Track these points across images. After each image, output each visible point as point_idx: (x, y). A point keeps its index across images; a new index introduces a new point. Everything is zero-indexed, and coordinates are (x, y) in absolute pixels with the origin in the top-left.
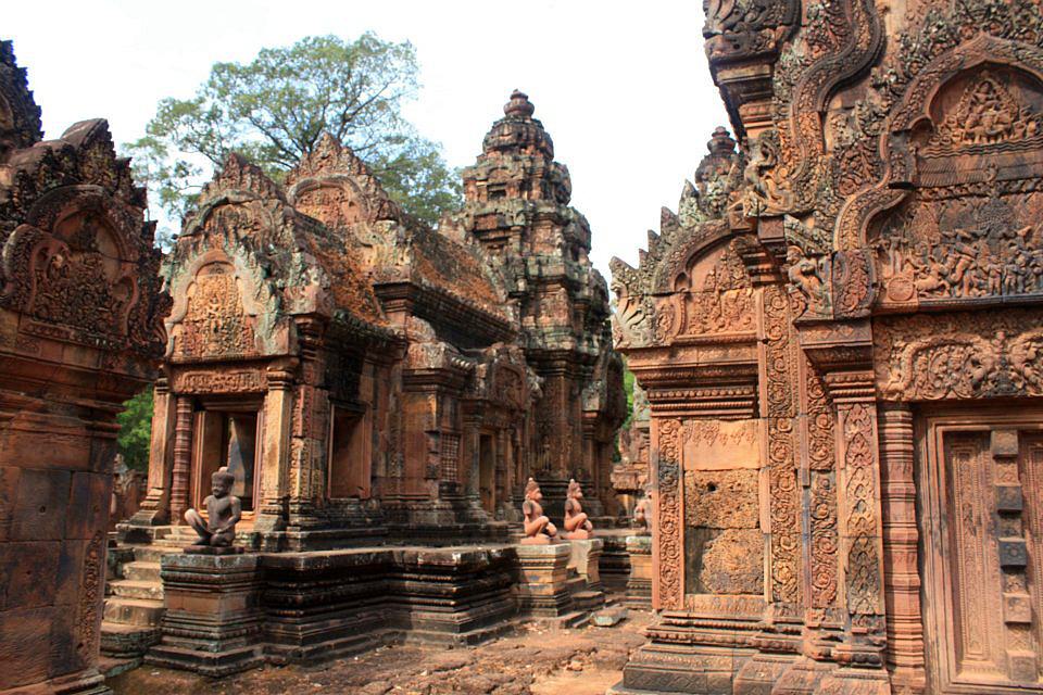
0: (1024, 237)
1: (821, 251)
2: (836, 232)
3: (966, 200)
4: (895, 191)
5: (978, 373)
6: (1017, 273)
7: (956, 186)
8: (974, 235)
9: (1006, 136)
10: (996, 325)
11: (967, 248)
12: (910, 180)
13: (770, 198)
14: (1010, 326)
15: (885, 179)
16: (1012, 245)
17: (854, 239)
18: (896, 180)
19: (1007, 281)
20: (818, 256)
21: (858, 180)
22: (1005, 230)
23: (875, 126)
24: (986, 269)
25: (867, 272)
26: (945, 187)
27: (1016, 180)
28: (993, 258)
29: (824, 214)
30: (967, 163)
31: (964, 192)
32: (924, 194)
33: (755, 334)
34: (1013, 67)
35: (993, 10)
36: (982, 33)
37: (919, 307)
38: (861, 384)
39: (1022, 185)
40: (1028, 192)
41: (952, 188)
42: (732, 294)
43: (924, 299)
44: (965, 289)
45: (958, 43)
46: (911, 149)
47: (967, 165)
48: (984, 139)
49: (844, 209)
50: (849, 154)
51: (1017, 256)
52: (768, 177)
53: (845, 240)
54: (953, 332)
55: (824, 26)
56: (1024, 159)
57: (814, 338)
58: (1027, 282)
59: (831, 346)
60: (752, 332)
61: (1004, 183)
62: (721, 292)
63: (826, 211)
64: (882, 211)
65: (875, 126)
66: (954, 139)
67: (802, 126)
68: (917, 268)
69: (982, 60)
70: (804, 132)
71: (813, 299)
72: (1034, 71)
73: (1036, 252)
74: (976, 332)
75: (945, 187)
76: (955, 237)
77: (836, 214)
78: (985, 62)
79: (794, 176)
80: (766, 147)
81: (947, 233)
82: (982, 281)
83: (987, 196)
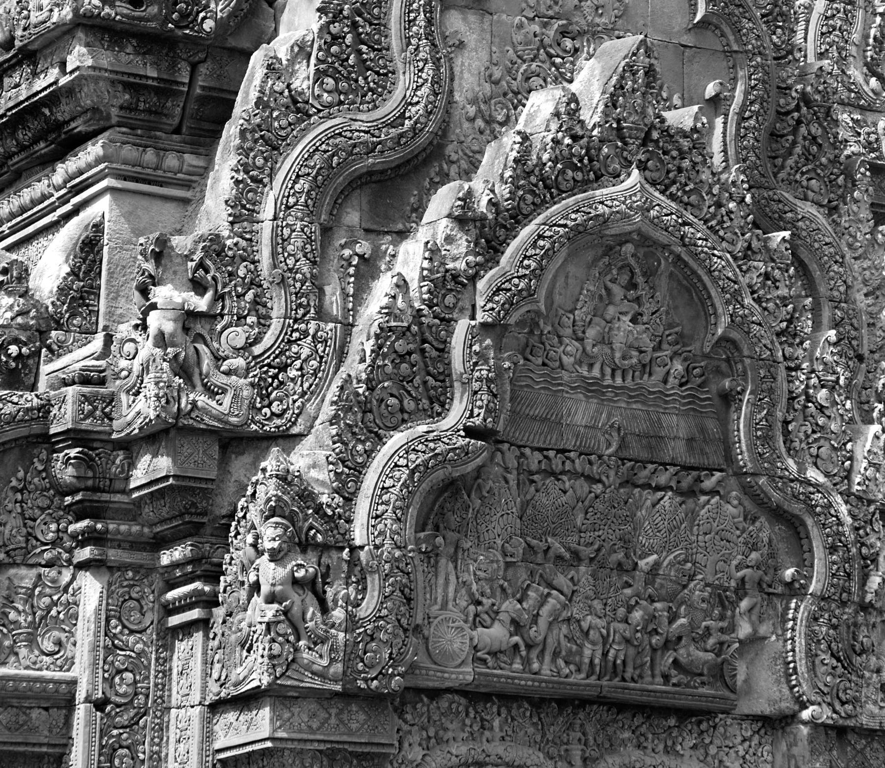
6: (628, 641)
7: (559, 451)
16: (628, 585)
18: (478, 421)
19: (612, 653)
21: (409, 404)
22: (620, 556)
24: (585, 625)
25: (409, 600)
26: (540, 450)
27: (644, 463)
30: (580, 412)
40: (658, 488)
41: (551, 454)
44: (547, 658)
51: (630, 609)
53: (380, 527)
59: (322, 747)
66: (565, 359)
73: (658, 605)
75: (540, 450)
76: (546, 551)
77: (364, 465)
82: (574, 647)
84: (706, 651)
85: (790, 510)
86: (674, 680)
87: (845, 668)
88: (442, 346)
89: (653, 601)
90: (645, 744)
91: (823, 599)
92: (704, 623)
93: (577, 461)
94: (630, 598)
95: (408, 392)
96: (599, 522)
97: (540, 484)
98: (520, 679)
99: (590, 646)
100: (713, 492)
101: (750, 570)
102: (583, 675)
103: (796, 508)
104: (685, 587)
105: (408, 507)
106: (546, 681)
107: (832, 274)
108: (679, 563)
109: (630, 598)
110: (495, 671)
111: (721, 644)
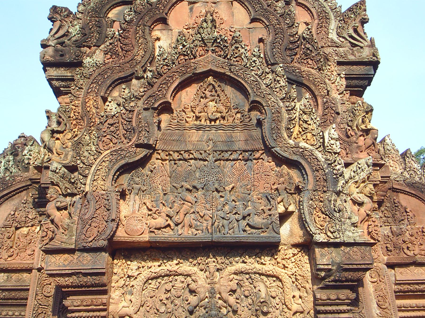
0: (230, 191)
1: (75, 191)
2: (90, 177)
3: (192, 161)
4: (138, 149)
5: (193, 300)
6: (223, 218)
7: (185, 151)
8: (194, 187)
9: (222, 121)
10: (209, 260)
11: (189, 197)
12: (151, 142)
13: (55, 153)
14: (220, 262)
15: (133, 141)
17: (102, 183)
18: (141, 142)
19: (216, 223)
20: (73, 195)
22: (216, 186)
23: (132, 104)
26: (178, 152)
27: (226, 151)
28: (208, 206)
29: (84, 163)
30: (195, 136)
31: (191, 156)
32: (162, 154)
33: (33, 264)
34: (227, 75)
35: (218, 41)
36: (210, 53)
37: (149, 242)
38: (95, 307)
39: (232, 154)
40: (234, 160)
41: (182, 152)
42: (25, 230)
43: (153, 235)
45: (195, 58)
46: (155, 121)
47: (194, 137)
48: (208, 122)
49: (98, 160)
50: (110, 121)
52: (58, 139)
54: (177, 264)
55: (116, 43)
56: (232, 137)
57: (58, 262)
58: (231, 226)
60: (32, 262)
61: (218, 152)
62: (17, 228)
63: (85, 161)
64: (127, 164)
65: (132, 104)
66: (187, 119)
67: (88, 105)
68: (150, 210)
69: (208, 69)
70: (88, 109)
71: (62, 230)
72: (240, 80)
73: (237, 203)
74: (195, 265)
75: (178, 152)
77: (93, 164)
78: (210, 70)
79: (76, 139)
80: (60, 117)
81: (175, 185)
82: (199, 223)
83: (206, 160)
84: (263, 219)
85: (293, 159)
86: (249, 232)
87: (331, 218)
88: (130, 120)
89: (235, 202)
90: (245, 261)
91: (314, 191)
92: (261, 208)
93: (194, 154)
94: (223, 202)
95: (114, 137)
96: (206, 174)
97: (178, 164)
98: (171, 238)
99: (205, 222)
100: (258, 159)
101: (280, 185)
102: (204, 234)
103: (295, 158)
104: (249, 194)
105: (108, 175)
106: (184, 238)
107: (320, 87)
108: (245, 186)
109: (223, 202)
110: (158, 236)
111: (270, 215)
